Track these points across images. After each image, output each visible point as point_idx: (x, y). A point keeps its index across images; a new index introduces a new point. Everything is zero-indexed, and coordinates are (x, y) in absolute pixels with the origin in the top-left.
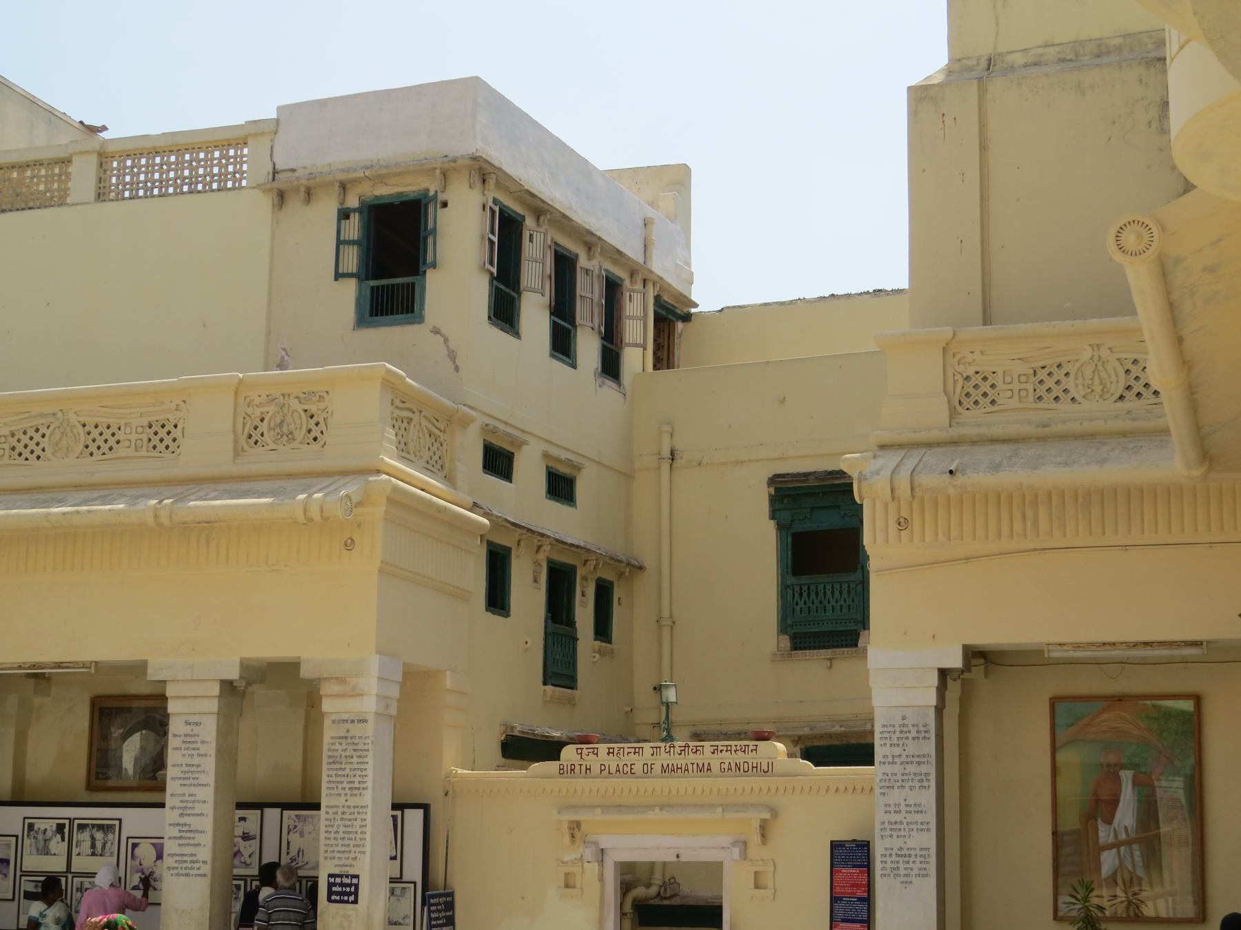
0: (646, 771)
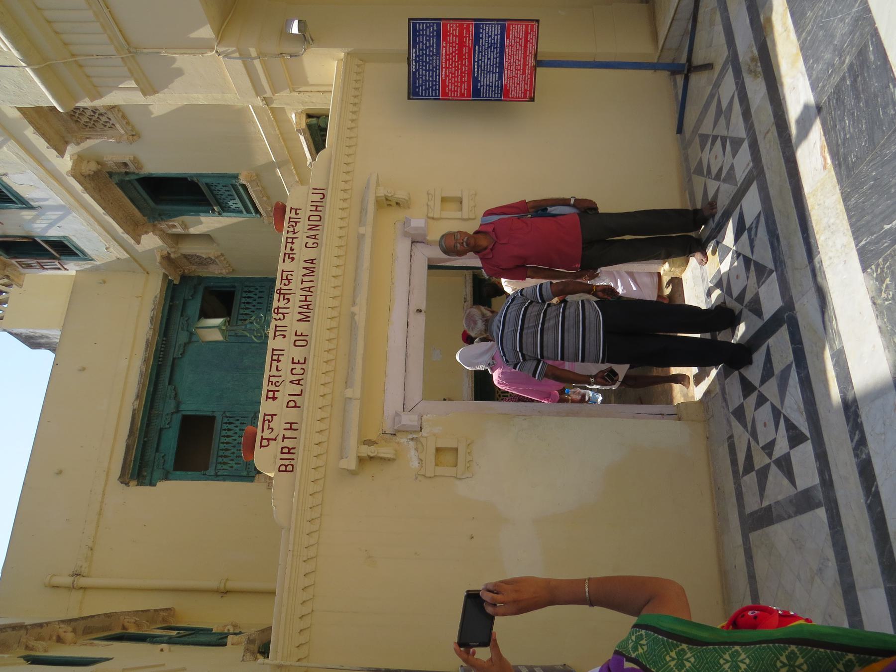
0: (304, 343)
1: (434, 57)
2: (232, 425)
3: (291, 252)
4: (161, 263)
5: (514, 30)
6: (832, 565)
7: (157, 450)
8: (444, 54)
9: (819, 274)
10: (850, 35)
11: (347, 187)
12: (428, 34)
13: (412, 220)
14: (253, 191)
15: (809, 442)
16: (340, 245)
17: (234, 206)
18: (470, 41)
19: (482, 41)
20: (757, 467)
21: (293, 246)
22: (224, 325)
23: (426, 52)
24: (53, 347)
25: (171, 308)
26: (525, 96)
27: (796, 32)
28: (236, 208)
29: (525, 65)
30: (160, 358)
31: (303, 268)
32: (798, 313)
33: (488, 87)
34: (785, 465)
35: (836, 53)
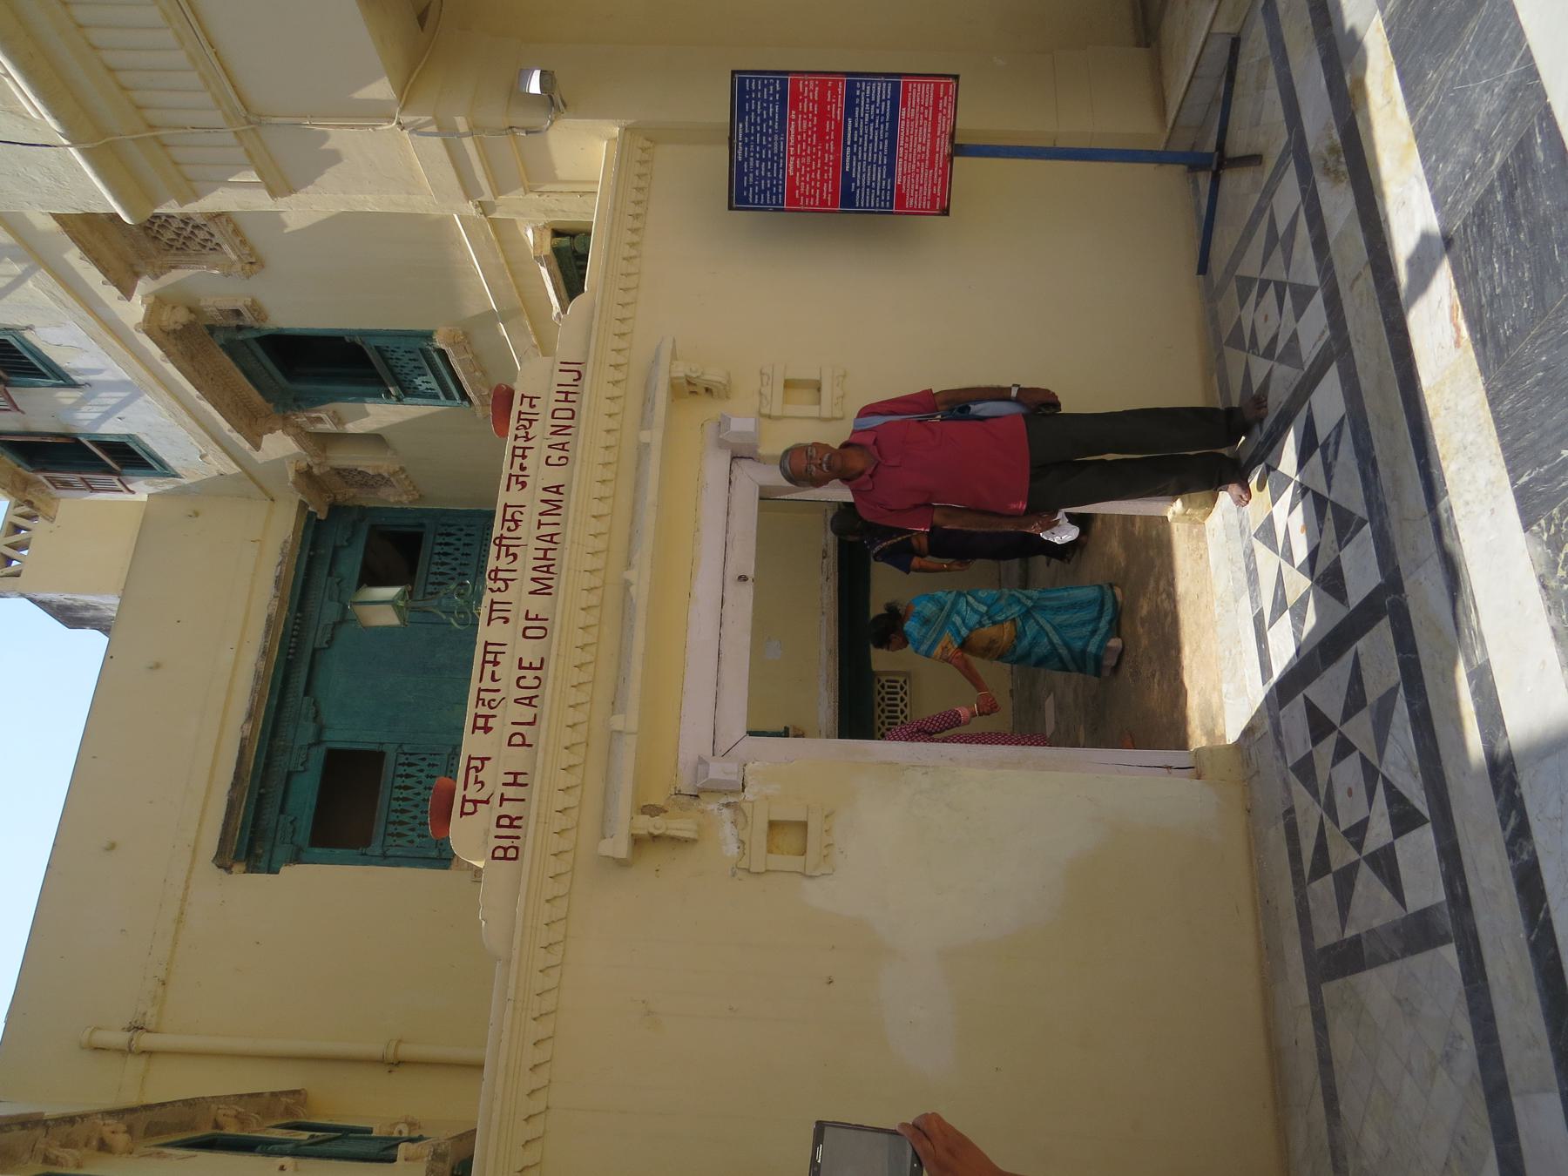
0: (540, 633)
1: (776, 137)
2: (405, 826)
3: (521, 473)
4: (295, 483)
5: (914, 94)
6: (1468, 1047)
7: (282, 811)
8: (793, 132)
9: (1447, 529)
10: (1503, 115)
11: (620, 359)
12: (765, 97)
13: (733, 419)
14: (459, 361)
15: (1429, 826)
16: (606, 461)
17: (425, 386)
18: (837, 111)
19: (860, 109)
20: (1335, 867)
21: (523, 461)
22: (402, 599)
23: (762, 128)
24: (105, 625)
25: (311, 560)
26: (933, 207)
27: (1409, 105)
28: (427, 389)
29: (933, 152)
30: (290, 648)
31: (542, 501)
32: (1408, 599)
33: (868, 190)
34: (1385, 864)
35: (1479, 145)
